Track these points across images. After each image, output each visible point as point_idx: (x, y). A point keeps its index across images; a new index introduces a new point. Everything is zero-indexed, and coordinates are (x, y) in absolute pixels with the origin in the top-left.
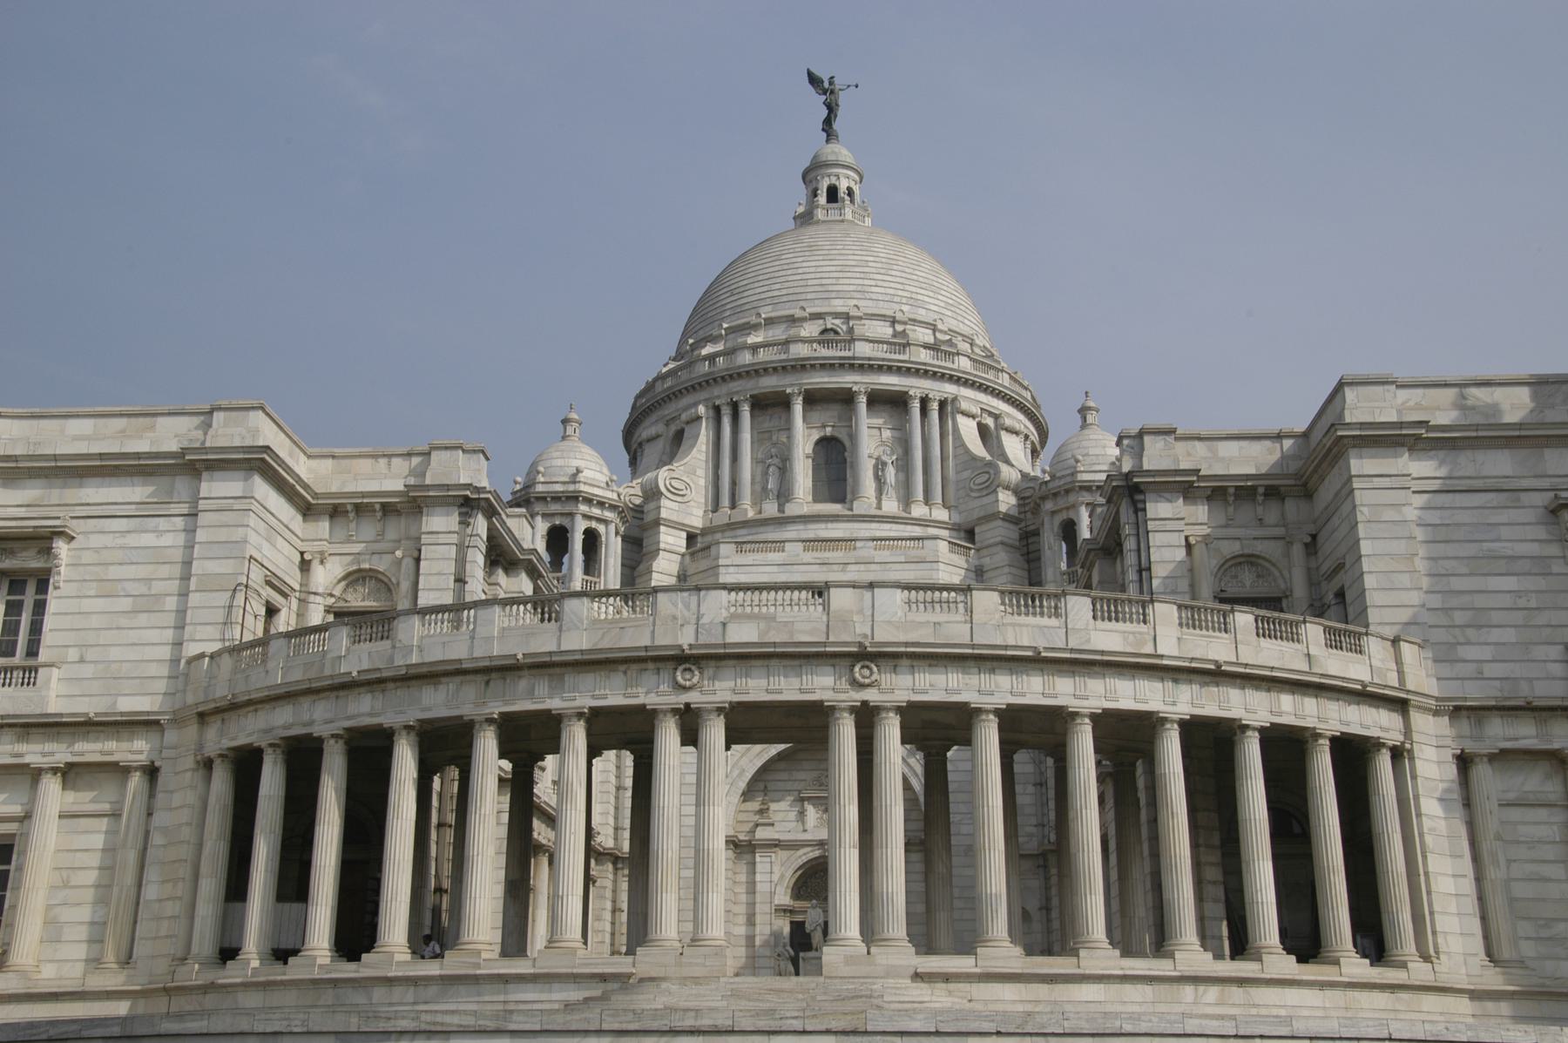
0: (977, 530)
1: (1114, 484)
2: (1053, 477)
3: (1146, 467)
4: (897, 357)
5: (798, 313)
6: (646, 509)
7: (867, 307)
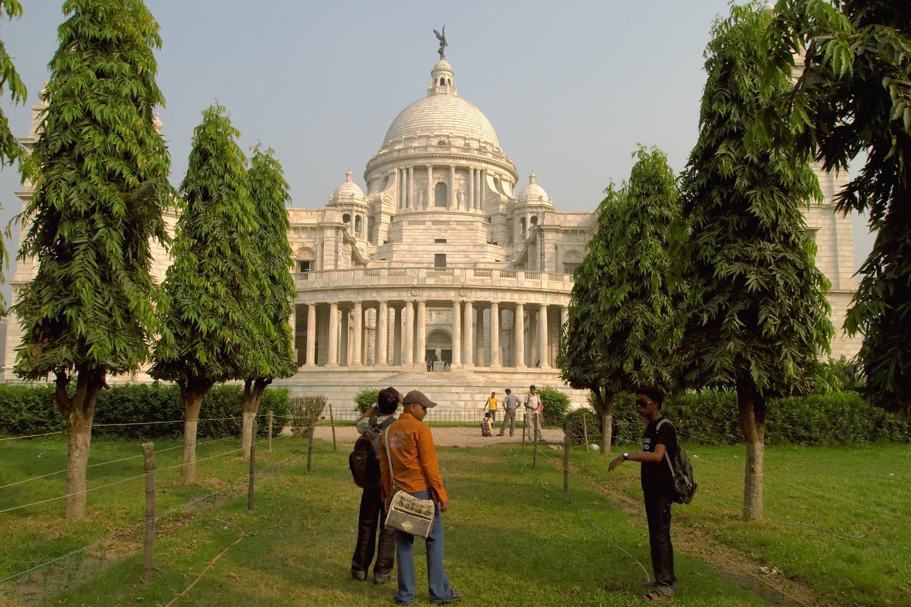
5: (431, 135)
7: (456, 133)
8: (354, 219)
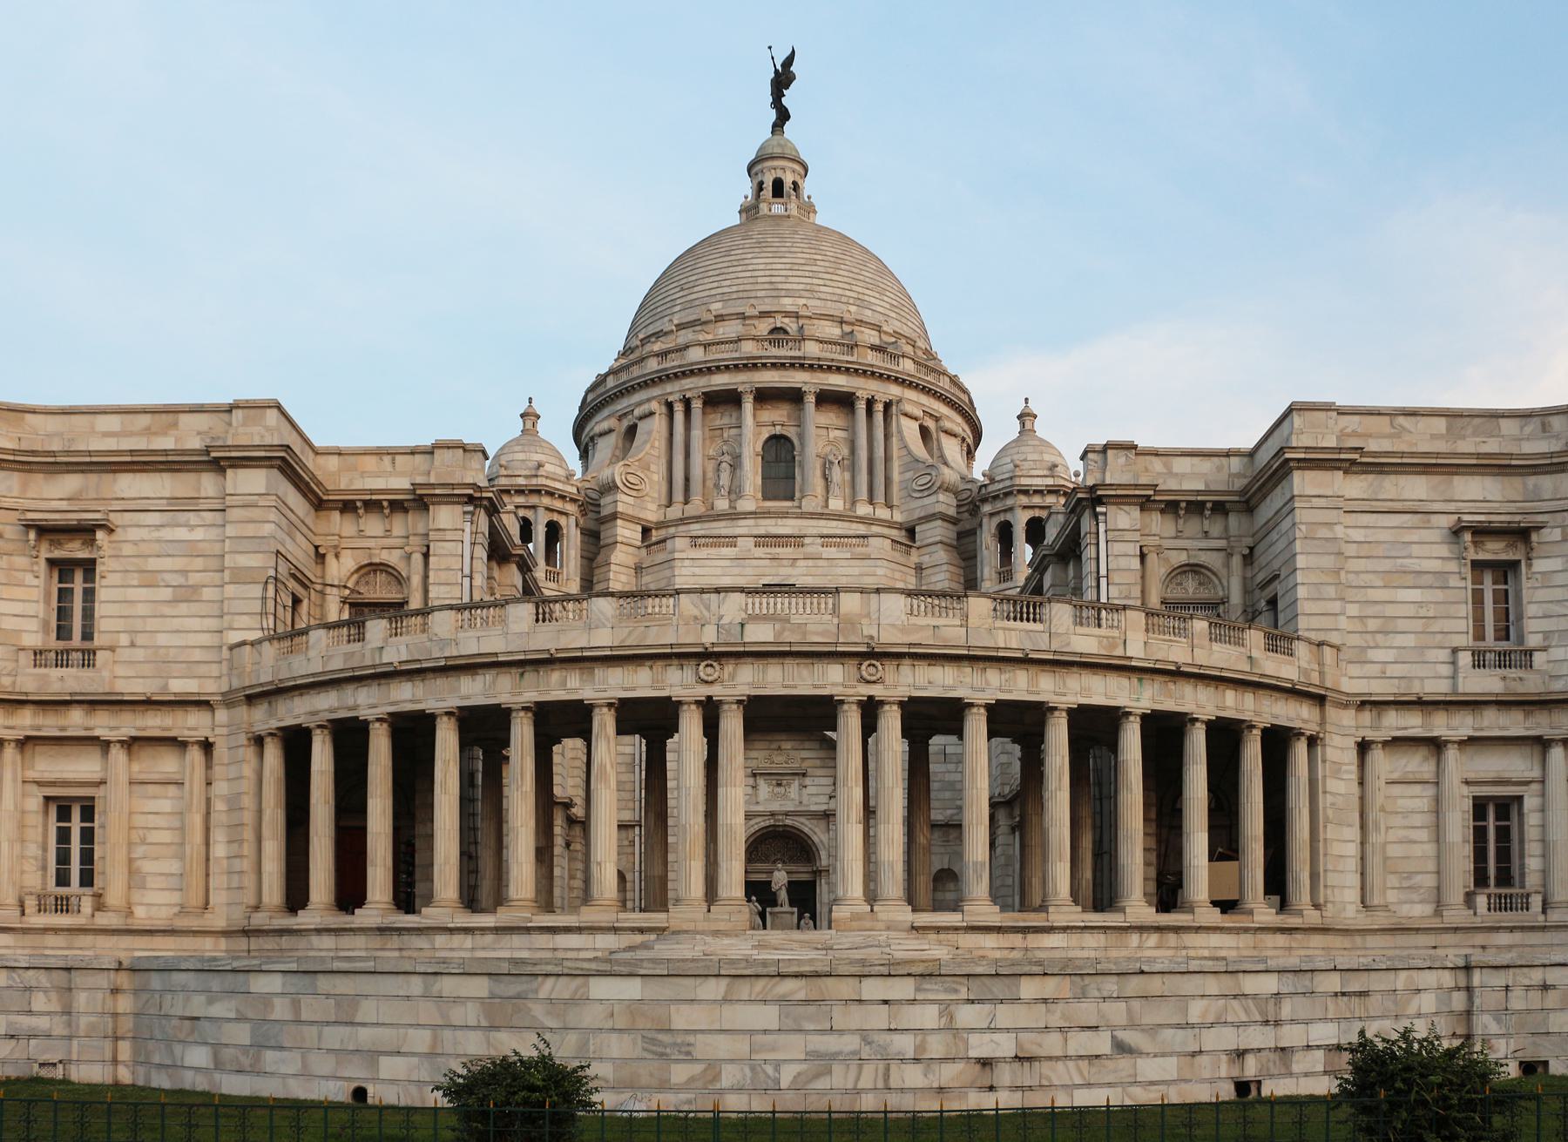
0: (918, 529)
1: (1080, 495)
2: (992, 481)
3: (1108, 482)
4: (846, 358)
5: (749, 312)
6: (602, 502)
7: (816, 306)
8: (540, 533)
